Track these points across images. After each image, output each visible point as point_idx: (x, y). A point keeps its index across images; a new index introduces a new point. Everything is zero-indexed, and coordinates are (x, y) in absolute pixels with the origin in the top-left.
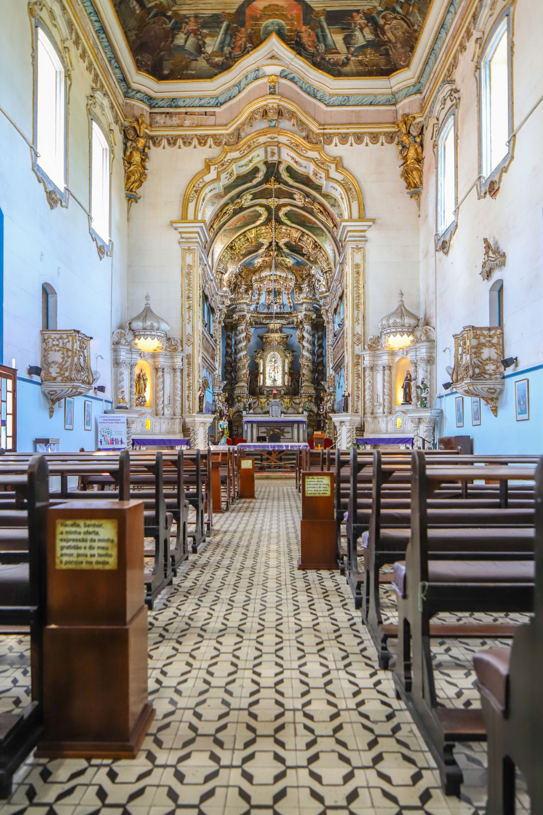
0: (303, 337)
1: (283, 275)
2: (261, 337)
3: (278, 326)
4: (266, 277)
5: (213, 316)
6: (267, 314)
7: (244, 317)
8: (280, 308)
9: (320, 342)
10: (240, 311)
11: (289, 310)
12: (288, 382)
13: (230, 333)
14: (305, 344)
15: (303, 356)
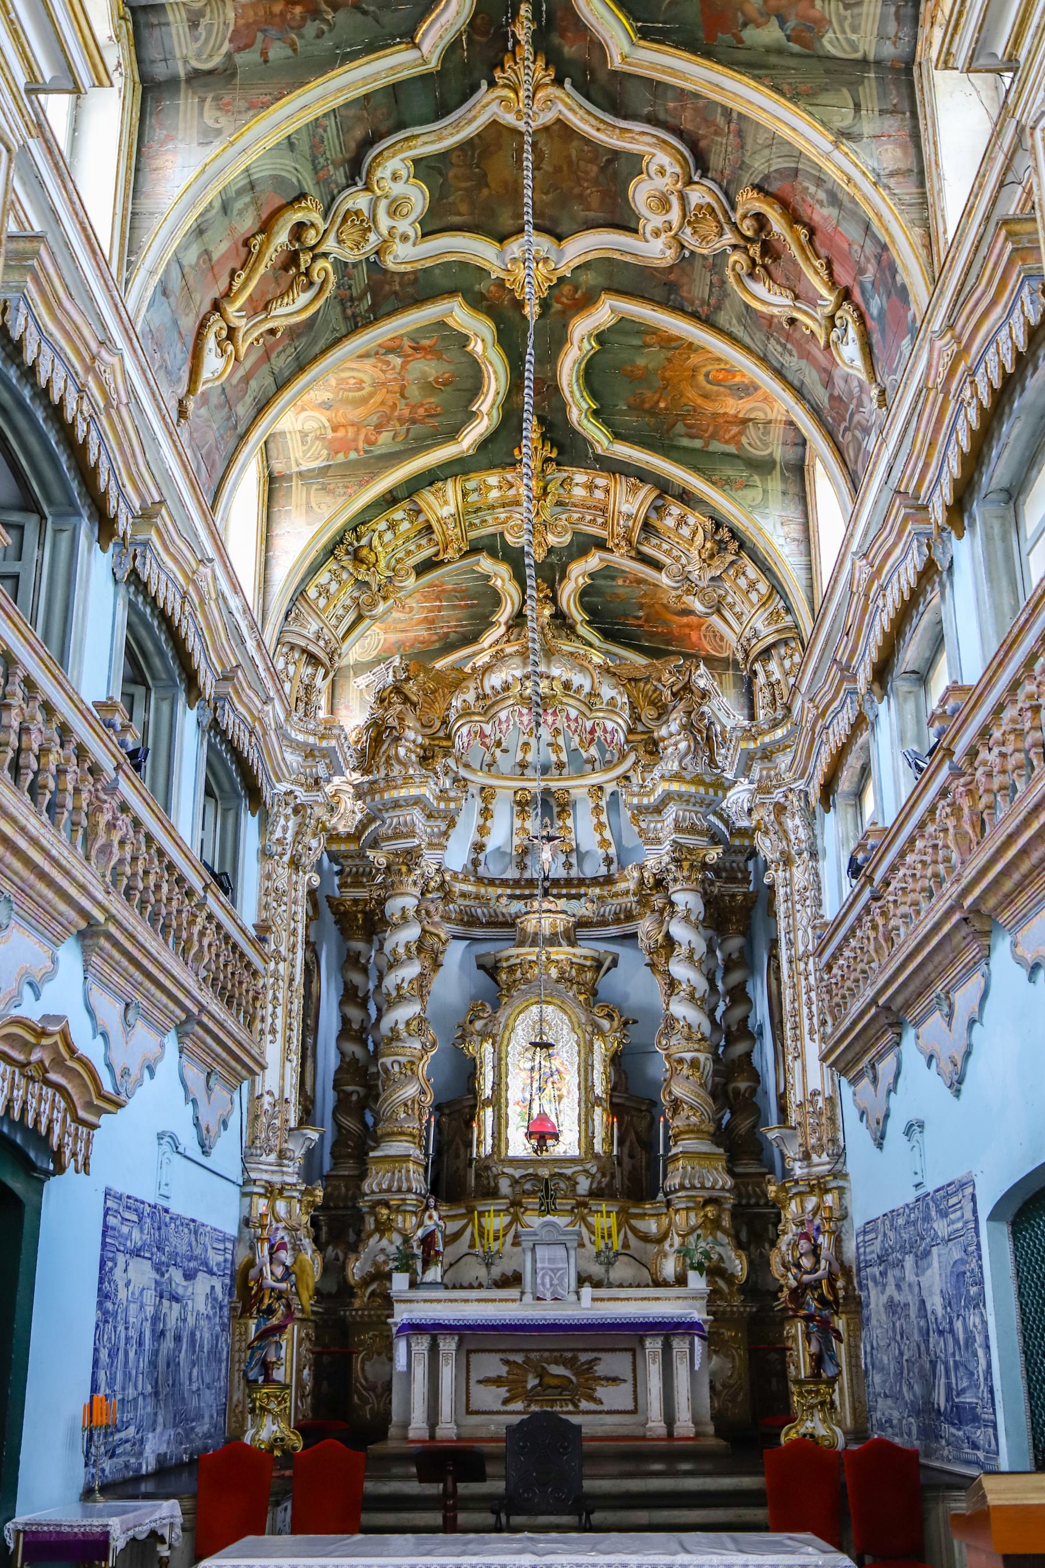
0: (670, 944)
1: (578, 679)
2: (490, 969)
3: (561, 923)
4: (506, 687)
5: (265, 824)
6: (516, 883)
7: (411, 857)
8: (568, 865)
9: (736, 977)
10: (397, 835)
11: (603, 870)
12: (608, 1140)
13: (359, 945)
14: (680, 970)
15: (671, 1021)
